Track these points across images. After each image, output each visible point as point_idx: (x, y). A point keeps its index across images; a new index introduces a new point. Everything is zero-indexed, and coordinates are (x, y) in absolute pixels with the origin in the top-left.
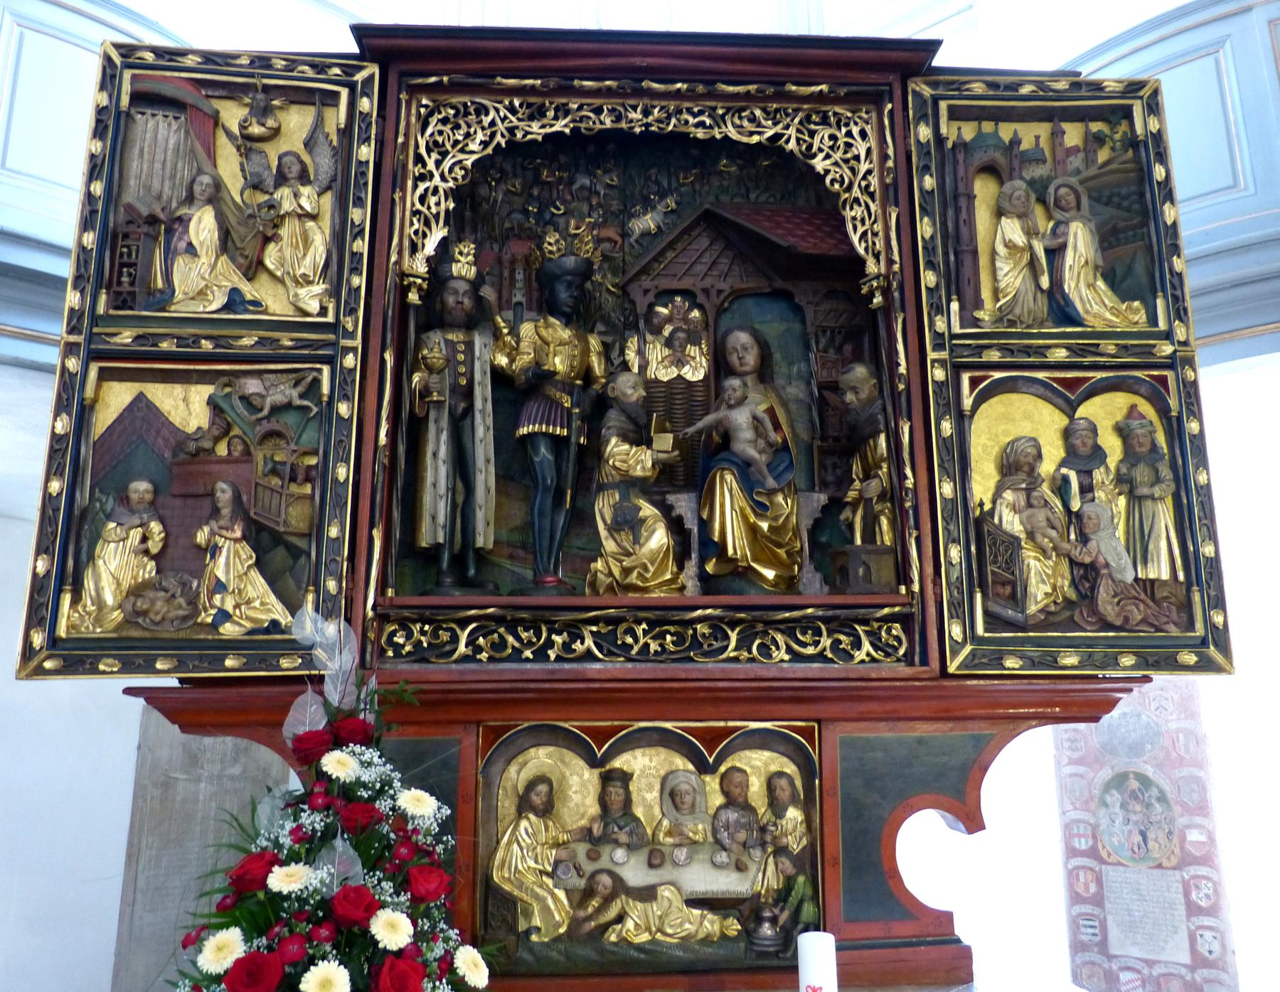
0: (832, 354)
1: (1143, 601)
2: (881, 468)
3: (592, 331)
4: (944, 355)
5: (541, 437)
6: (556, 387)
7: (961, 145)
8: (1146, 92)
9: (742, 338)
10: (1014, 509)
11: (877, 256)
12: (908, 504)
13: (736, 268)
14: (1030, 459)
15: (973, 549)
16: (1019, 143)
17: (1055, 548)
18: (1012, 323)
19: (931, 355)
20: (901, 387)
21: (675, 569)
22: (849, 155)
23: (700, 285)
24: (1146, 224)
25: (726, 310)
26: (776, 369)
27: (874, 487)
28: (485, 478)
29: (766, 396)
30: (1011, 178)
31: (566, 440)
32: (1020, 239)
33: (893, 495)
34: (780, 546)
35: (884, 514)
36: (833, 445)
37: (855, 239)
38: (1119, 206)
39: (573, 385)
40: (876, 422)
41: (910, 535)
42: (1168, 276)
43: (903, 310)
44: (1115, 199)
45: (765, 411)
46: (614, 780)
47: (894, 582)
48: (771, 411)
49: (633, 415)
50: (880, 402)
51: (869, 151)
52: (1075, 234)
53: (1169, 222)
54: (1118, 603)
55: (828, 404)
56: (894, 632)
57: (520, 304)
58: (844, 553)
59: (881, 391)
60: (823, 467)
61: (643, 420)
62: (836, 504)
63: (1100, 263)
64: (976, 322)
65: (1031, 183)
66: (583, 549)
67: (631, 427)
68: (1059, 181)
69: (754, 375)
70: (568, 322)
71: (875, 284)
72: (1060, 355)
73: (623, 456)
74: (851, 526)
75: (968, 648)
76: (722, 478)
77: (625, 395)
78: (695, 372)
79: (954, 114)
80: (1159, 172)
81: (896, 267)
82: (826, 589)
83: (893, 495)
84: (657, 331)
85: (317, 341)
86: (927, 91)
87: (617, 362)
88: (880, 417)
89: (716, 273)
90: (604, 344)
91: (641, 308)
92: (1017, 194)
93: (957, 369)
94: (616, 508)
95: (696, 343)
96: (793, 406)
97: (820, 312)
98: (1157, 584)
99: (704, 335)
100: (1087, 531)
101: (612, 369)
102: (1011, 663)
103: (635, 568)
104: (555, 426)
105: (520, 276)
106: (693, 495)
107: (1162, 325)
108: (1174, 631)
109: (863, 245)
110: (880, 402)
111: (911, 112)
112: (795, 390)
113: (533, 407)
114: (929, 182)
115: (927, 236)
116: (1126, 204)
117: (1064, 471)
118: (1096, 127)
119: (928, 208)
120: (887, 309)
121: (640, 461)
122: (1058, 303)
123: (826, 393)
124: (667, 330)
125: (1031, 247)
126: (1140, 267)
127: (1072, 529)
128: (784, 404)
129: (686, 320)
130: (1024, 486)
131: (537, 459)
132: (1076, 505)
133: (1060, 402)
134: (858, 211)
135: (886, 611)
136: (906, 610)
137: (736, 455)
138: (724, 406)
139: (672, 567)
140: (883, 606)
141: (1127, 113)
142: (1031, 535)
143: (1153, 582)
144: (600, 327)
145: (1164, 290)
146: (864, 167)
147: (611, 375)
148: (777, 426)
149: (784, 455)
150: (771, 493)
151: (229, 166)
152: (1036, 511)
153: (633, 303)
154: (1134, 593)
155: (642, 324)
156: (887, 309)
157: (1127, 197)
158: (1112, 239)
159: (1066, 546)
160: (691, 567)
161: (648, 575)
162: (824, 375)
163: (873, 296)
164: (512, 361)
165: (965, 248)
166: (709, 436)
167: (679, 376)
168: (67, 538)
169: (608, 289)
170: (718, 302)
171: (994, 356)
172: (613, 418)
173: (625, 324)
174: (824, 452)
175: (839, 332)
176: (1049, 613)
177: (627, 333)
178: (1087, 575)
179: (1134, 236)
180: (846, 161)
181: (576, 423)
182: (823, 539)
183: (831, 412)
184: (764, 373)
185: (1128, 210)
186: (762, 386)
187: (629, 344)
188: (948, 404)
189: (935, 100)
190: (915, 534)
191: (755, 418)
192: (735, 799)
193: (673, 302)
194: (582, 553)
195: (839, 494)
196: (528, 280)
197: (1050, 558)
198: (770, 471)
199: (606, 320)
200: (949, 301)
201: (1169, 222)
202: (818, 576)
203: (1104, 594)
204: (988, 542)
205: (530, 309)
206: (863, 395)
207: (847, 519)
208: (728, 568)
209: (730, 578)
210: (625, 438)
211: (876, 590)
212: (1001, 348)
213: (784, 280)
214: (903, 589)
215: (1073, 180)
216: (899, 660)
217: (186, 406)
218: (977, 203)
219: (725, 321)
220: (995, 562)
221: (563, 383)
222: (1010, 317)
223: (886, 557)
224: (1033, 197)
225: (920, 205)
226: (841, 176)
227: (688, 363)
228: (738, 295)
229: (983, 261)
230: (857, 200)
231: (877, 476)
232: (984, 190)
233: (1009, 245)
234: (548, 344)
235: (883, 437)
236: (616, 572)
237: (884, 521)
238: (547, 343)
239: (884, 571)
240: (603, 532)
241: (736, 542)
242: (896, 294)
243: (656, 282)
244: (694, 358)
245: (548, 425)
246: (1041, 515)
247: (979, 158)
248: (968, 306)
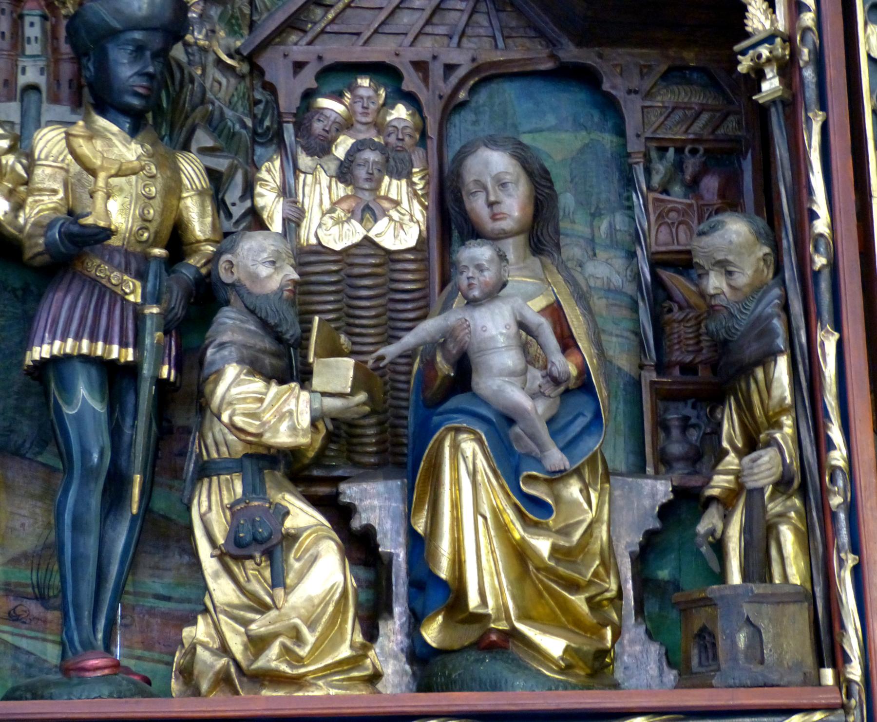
0: (677, 195)
2: (779, 426)
3: (186, 147)
5: (79, 367)
6: (110, 262)
9: (495, 162)
12: (836, 501)
13: (481, 19)
20: (820, 261)
21: (359, 638)
23: (412, 54)
25: (463, 105)
26: (564, 225)
27: (766, 466)
29: (544, 280)
31: (132, 370)
33: (804, 482)
34: (574, 587)
35: (788, 521)
36: (689, 379)
39: (147, 258)
40: (767, 332)
41: (841, 562)
43: (823, 105)
45: (542, 312)
47: (810, 660)
48: (555, 312)
49: (272, 321)
50: (777, 291)
55: (670, 297)
57: (33, 88)
58: (708, 602)
59: (779, 270)
60: (662, 425)
61: (291, 331)
62: (687, 503)
66: (168, 599)
67: (267, 343)
69: (521, 239)
70: (136, 124)
73: (254, 406)
74: (719, 547)
76: (456, 447)
77: (255, 277)
81: (808, 19)
82: (671, 676)
83: (804, 482)
84: (321, 148)
87: (237, 212)
88: (778, 324)
89: (442, 30)
90: (212, 174)
91: (288, 101)
94: (234, 510)
95: (402, 172)
96: (599, 303)
97: (657, 109)
99: (417, 155)
101: (228, 226)
103: (275, 635)
104: (108, 341)
105: (33, 31)
106: (396, 485)
110: (777, 291)
112: (606, 270)
113: (60, 303)
120: (790, 104)
121: (287, 416)
123: (666, 275)
124: (342, 146)
128: (582, 298)
129: (379, 126)
131: (69, 411)
137: (485, 402)
138: (459, 301)
139: (352, 633)
144: (203, 138)
147: (225, 238)
148: (567, 343)
149: (581, 401)
150: (557, 478)
153: (270, 88)
155: (289, 132)
156: (790, 104)
160: (393, 633)
161: (303, 652)
162: (661, 239)
163: (760, 75)
164: (18, 207)
166: (429, 364)
167: (366, 238)
169: (219, 61)
170: (446, 89)
172: (231, 326)
173: (255, 133)
174: (666, 396)
175: (694, 152)
177: (259, 151)
181: (153, 337)
182: (664, 574)
183: (677, 315)
184: (541, 233)
186: (535, 262)
187: (264, 174)
190: (851, 560)
191: (522, 325)
193: (352, 88)
194: (163, 606)
195: (694, 481)
196: (50, 37)
198: (553, 435)
199: (215, 124)
202: (655, 649)
205: (55, 99)
206: (742, 279)
207: (712, 532)
208: (471, 634)
209: (473, 655)
210: (254, 366)
211: (774, 677)
213: (579, 44)
214: (828, 675)
219: (462, 127)
221: (127, 254)
223: (792, 608)
227: (385, 213)
228: (486, 76)
231: (771, 442)
234: (93, 172)
235: (782, 365)
236: (236, 644)
237: (788, 536)
239: (791, 639)
240: (209, 563)
241: (487, 583)
242: (809, 74)
243: (317, 48)
244: (397, 203)
245: (93, 339)
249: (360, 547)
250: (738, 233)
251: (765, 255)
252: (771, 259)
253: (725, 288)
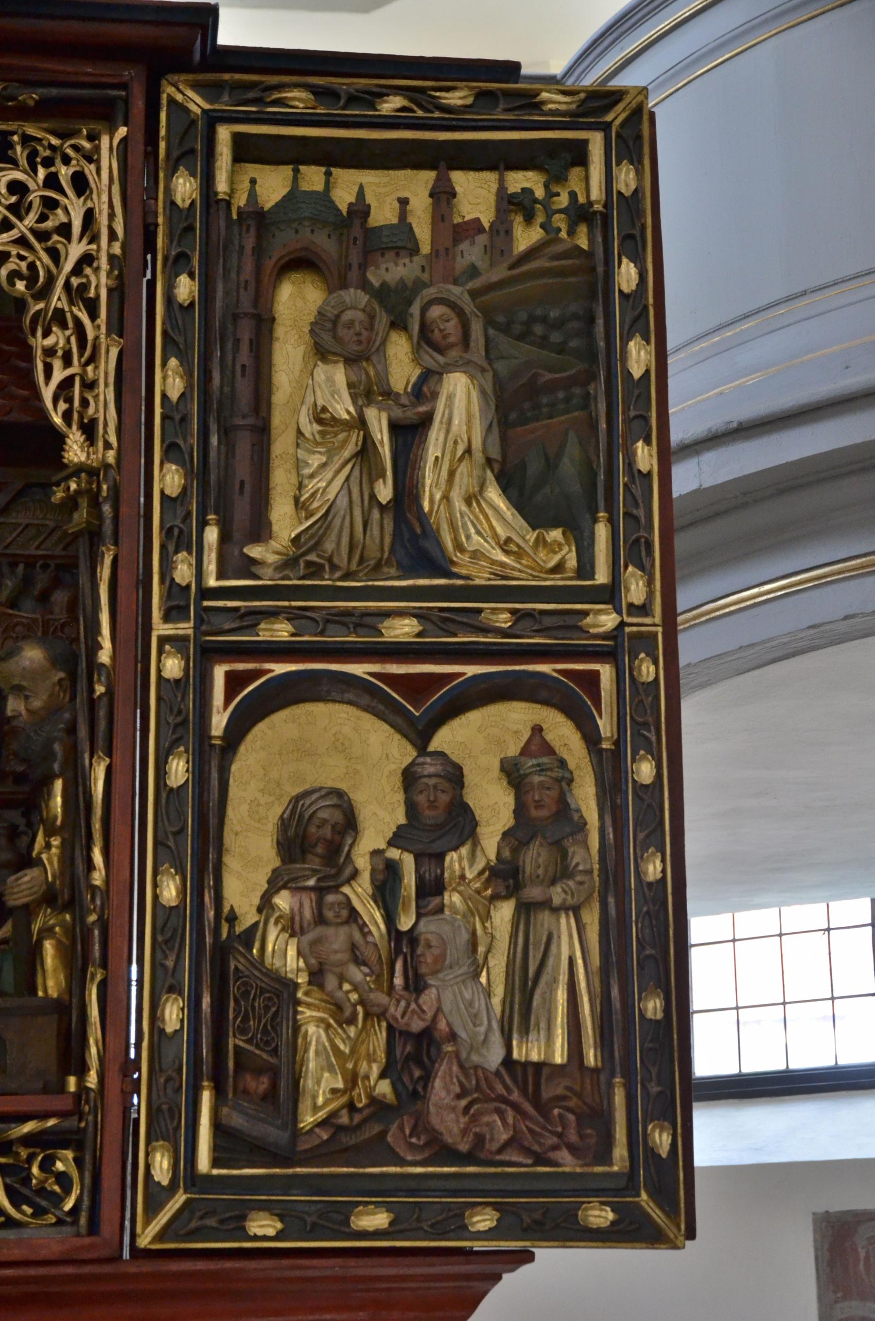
1: (515, 1106)
4: (185, 628)
7: (258, 218)
8: (617, 116)
10: (292, 927)
11: (89, 430)
14: (327, 832)
15: (206, 1001)
16: (365, 212)
17: (362, 1002)
18: (315, 570)
19: (160, 628)
22: (49, 224)
24: (594, 377)
30: (344, 286)
32: (343, 407)
37: (48, 393)
38: (543, 343)
40: (52, 755)
42: (622, 480)
44: (538, 329)
51: (89, 217)
52: (450, 398)
53: (637, 372)
54: (467, 1109)
56: (60, 1166)
63: (495, 453)
64: (248, 567)
65: (382, 294)
68: (430, 292)
71: (73, 486)
72: (403, 630)
75: (180, 1198)
79: (246, 151)
80: (627, 275)
86: (197, 103)
92: (348, 315)
93: (207, 654)
98: (545, 1071)
100: (423, 969)
102: (263, 1227)
107: (602, 577)
108: (568, 1163)
109: (62, 406)
110: (67, 716)
111: (162, 145)
114: (186, 288)
115: (174, 395)
116: (556, 337)
117: (394, 853)
118: (520, 180)
119: (180, 340)
120: (93, 536)
122: (412, 530)
125: (361, 423)
126: (569, 467)
127: (399, 966)
130: (311, 882)
132: (406, 923)
133: (399, 721)
134: (57, 338)
135: (28, 1127)
136: (72, 1123)
140: (24, 1118)
141: (578, 155)
142: (316, 976)
143: (539, 1066)
145: (611, 509)
146: (76, 250)
152: (330, 931)
154: (500, 1089)
157: (559, 324)
158: (527, 405)
159: (381, 998)
165: (239, 421)
171: (281, 631)
175: (45, 567)
176: (340, 1128)
178: (416, 1052)
179: (567, 400)
180: (42, 236)
185: (561, 349)
188: (184, 723)
189: (213, 120)
197: (352, 1021)
200: (203, 524)
201: (637, 372)
203: (441, 1090)
204: (233, 989)
212: (292, 615)
214: (72, 1083)
215: (456, 292)
216: (60, 1222)
218: (280, 331)
220: (243, 1030)
222: (312, 557)
224: (383, 319)
225: (165, 333)
226: (32, 267)
229: (282, 445)
230: (59, 317)
232: (297, 302)
233: (320, 416)
235: (58, 785)
237: (49, 947)
239: (40, 1047)
242: (107, 509)
246: (338, 939)
247: (284, 242)
248: (237, 535)
250: (32, 660)
251: (61, 680)
252: (67, 683)
253: (24, 712)
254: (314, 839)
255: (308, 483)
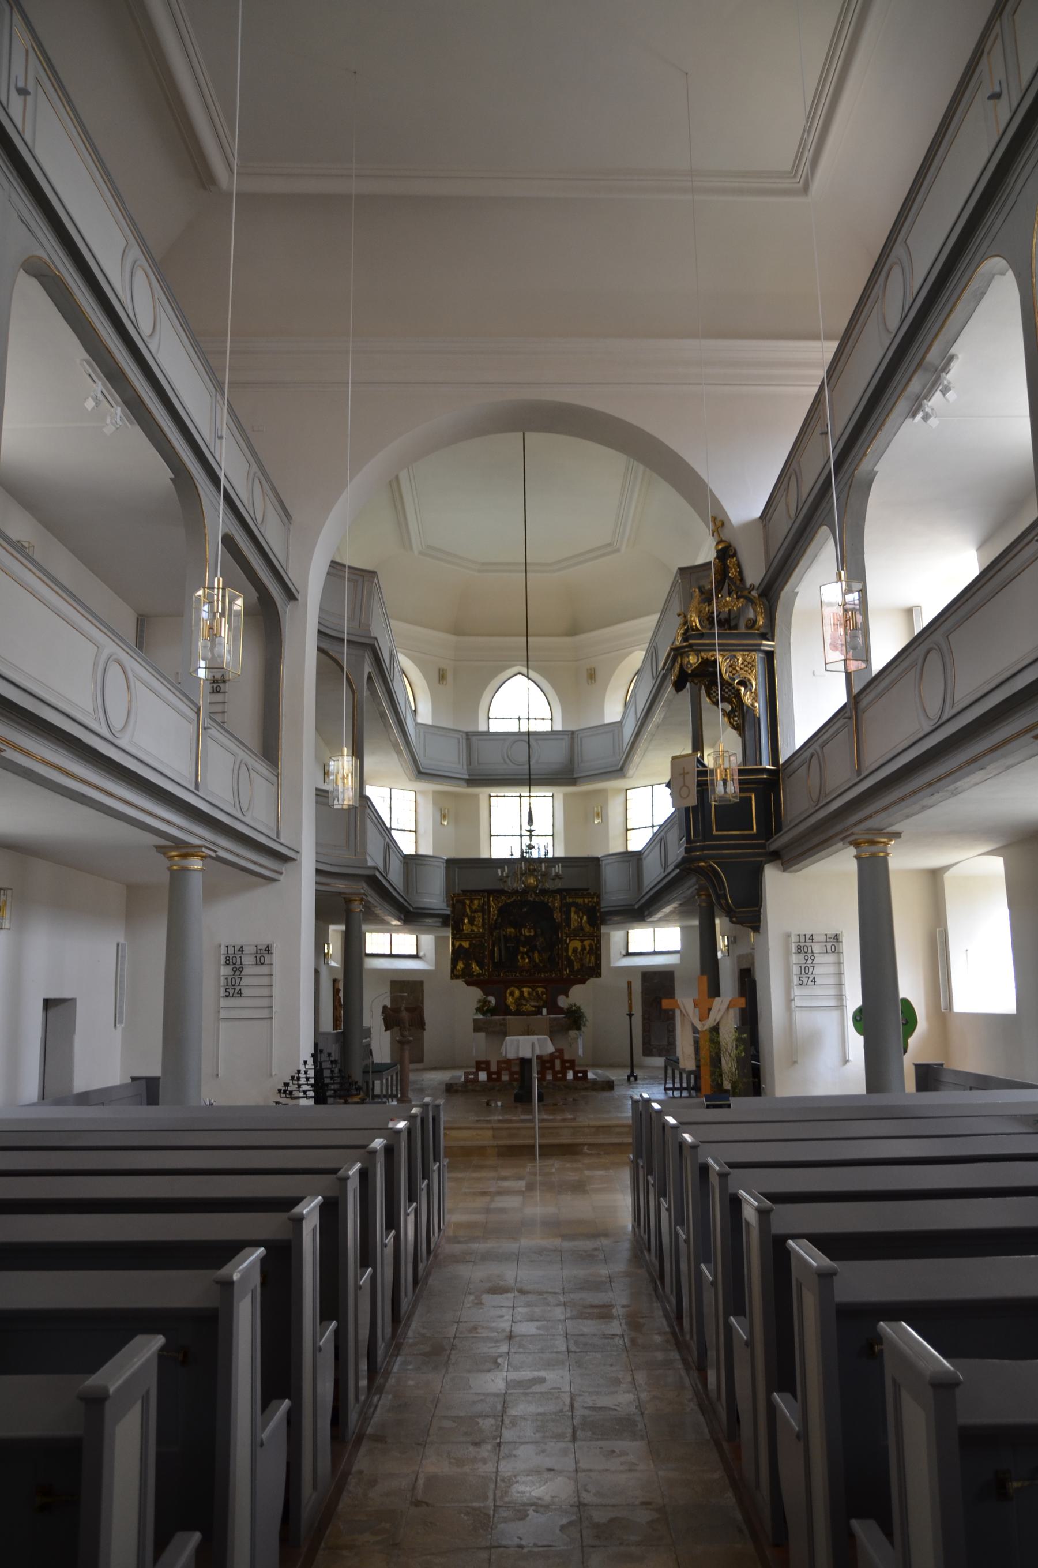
28: (503, 952)
46: (522, 993)
78: (532, 934)
85: (482, 935)
151: (468, 910)
168: (454, 962)
192: (537, 994)
217: (466, 945)
232: (573, 909)
238: (511, 930)
249: (529, 958)
254: (575, 950)
255: (574, 924)
